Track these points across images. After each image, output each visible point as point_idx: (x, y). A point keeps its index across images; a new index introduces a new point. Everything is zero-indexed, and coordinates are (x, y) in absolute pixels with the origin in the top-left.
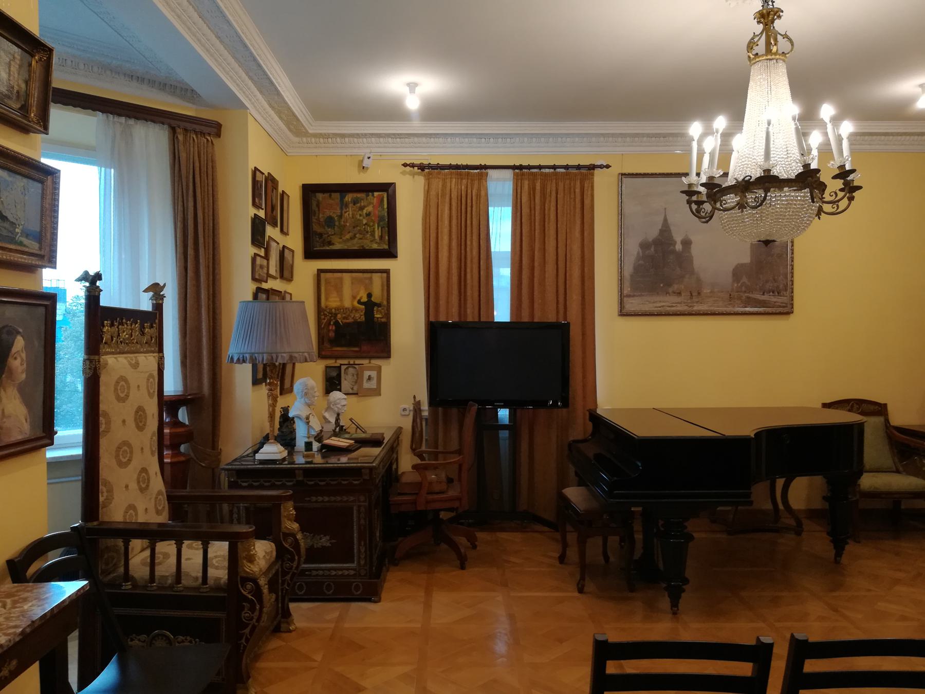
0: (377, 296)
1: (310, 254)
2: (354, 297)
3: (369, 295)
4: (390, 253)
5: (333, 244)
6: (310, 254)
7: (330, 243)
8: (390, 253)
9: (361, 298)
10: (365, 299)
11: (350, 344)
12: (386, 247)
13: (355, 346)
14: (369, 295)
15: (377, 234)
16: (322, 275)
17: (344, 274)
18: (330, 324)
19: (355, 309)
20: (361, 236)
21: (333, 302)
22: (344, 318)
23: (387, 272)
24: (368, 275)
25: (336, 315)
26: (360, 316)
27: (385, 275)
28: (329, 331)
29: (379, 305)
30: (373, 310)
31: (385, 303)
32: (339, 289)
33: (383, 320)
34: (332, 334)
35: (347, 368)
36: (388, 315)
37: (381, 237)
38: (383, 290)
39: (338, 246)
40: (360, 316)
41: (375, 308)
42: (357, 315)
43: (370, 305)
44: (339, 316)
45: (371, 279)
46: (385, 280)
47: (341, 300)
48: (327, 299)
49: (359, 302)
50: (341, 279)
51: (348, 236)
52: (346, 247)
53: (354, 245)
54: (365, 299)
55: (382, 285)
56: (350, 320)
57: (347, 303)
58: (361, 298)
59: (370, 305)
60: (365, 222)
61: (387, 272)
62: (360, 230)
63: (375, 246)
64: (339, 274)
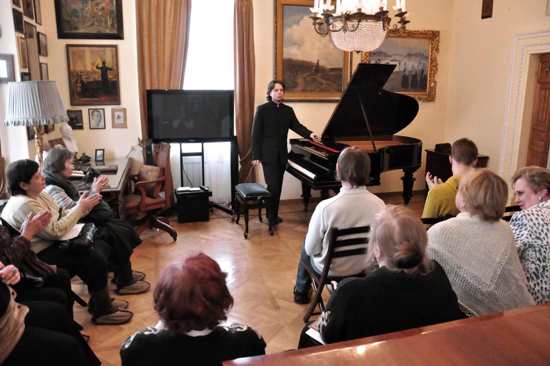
1: (62, 35)
2: (93, 64)
3: (104, 63)
4: (119, 36)
5: (78, 29)
6: (62, 35)
7: (76, 28)
8: (119, 36)
9: (98, 64)
10: (101, 65)
11: (92, 96)
12: (116, 32)
13: (95, 97)
14: (104, 63)
15: (109, 23)
16: (70, 48)
17: (86, 48)
18: (77, 82)
19: (94, 72)
21: (79, 68)
23: (116, 47)
25: (81, 76)
26: (98, 77)
27: (114, 49)
29: (111, 69)
31: (115, 68)
32: (81, 57)
33: (114, 79)
34: (79, 89)
35: (93, 112)
36: (117, 75)
37: (112, 25)
38: (113, 59)
39: (81, 31)
40: (98, 77)
41: (108, 72)
42: (96, 76)
43: (104, 70)
44: (83, 77)
45: (104, 51)
46: (114, 52)
47: (85, 66)
48: (74, 65)
49: (97, 67)
50: (83, 52)
51: (89, 24)
52: (87, 32)
54: (101, 65)
55: (113, 55)
56: (91, 80)
57: (89, 68)
58: (98, 64)
59: (104, 70)
60: (100, 14)
61: (116, 47)
63: (108, 31)
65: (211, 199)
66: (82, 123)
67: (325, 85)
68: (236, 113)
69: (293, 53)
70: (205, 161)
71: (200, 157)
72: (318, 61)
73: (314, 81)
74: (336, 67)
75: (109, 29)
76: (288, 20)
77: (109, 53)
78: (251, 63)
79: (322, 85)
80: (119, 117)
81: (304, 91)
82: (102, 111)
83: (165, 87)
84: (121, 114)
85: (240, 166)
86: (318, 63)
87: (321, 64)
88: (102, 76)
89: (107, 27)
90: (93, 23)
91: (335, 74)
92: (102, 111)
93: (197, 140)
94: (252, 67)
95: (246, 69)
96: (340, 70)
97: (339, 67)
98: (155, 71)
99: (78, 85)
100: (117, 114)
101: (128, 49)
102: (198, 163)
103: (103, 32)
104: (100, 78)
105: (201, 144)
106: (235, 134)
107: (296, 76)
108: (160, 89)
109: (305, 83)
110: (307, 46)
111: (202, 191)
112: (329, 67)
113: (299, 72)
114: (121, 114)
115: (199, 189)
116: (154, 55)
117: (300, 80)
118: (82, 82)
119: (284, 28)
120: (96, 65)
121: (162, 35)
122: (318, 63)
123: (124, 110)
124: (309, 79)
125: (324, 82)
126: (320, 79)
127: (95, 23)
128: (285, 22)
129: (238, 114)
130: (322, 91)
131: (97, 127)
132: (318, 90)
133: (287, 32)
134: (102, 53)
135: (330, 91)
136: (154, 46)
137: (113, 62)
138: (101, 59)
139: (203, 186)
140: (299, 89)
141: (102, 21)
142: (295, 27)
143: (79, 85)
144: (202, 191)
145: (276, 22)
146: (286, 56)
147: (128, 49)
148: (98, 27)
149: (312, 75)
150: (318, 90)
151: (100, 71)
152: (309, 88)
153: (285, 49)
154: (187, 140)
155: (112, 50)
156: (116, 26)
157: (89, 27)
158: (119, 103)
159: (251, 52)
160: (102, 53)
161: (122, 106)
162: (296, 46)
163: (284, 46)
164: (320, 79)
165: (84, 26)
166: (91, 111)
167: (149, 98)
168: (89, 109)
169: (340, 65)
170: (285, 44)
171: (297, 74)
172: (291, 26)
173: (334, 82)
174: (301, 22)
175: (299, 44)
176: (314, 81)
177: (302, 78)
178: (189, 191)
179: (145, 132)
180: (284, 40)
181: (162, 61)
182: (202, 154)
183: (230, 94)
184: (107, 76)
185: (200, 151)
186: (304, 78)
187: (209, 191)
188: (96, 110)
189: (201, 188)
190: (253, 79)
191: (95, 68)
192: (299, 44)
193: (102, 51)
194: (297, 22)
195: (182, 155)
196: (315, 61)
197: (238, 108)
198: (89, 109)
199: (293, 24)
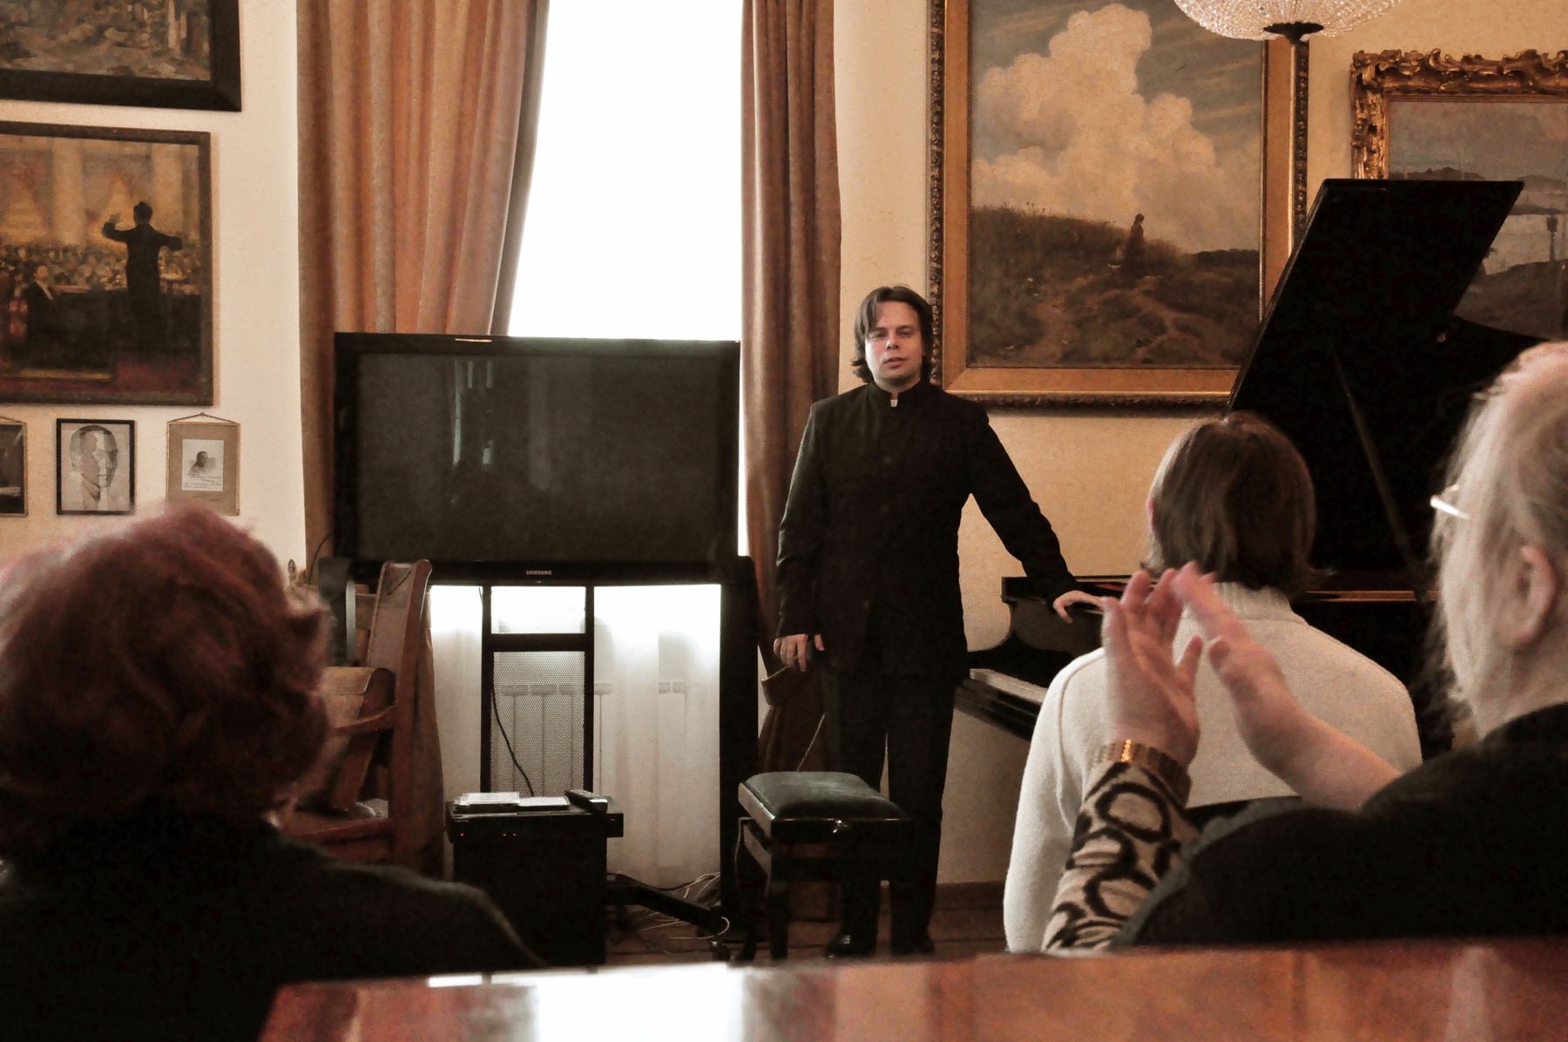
0: (168, 216)
2: (91, 216)
3: (143, 212)
5: (27, 55)
7: (15, 50)
8: (222, 92)
10: (127, 223)
12: (204, 75)
14: (143, 212)
15: (175, 34)
17: (59, 142)
19: (91, 252)
20: (121, 37)
22: (58, 279)
23: (201, 141)
24: (140, 148)
25: (31, 267)
26: (110, 274)
27: (193, 150)
28: (8, 317)
29: (174, 243)
30: (155, 258)
31: (194, 236)
33: (188, 289)
34: (18, 328)
36: (203, 271)
37: (188, 46)
38: (185, 198)
39: (40, 63)
40: (110, 274)
41: (163, 253)
42: (104, 273)
43: (144, 243)
44: (42, 271)
45: (148, 157)
46: (194, 168)
47: (49, 222)
49: (110, 231)
50: (47, 157)
51: (76, 33)
52: (69, 68)
53: (100, 63)
54: (127, 223)
55: (185, 180)
56: (80, 286)
57: (70, 236)
59: (144, 243)
61: (201, 141)
62: (116, 17)
63: (167, 71)
64: (42, 142)
65: (623, 855)
66: (21, 482)
67: (1173, 333)
68: (750, 454)
69: (1015, 182)
70: (598, 681)
71: (577, 657)
72: (1139, 218)
73: (1121, 311)
74: (1227, 249)
75: (172, 61)
76: (992, 35)
77: (168, 165)
78: (823, 224)
79: (1162, 329)
80: (201, 461)
81: (1073, 358)
82: (121, 433)
83: (419, 321)
84: (214, 448)
85: (764, 709)
86: (1137, 229)
87: (1158, 230)
88: (129, 269)
89: (162, 53)
90: (100, 31)
91: (1225, 280)
92: (121, 433)
93: (561, 575)
94: (825, 242)
95: (796, 252)
96: (1247, 259)
97: (1241, 247)
98: (378, 253)
99: (13, 308)
100: (191, 448)
101: (257, 155)
102: (566, 691)
103: (144, 74)
104: (122, 280)
105: (580, 591)
106: (743, 549)
107: (1030, 291)
108: (401, 329)
109: (1079, 325)
110: (1087, 150)
111: (576, 811)
112: (1189, 246)
113: (1047, 273)
114: (214, 448)
115: (562, 801)
116: (377, 179)
117: (1052, 311)
118: (34, 294)
119: (978, 65)
120: (105, 218)
121: (416, 91)
122: (1137, 229)
123: (230, 433)
124: (1093, 302)
125: (1168, 316)
126: (1149, 306)
127: (109, 33)
128: (981, 42)
129: (760, 455)
130: (1161, 358)
131: (92, 506)
132: (1141, 353)
133: (993, 84)
134: (135, 169)
135: (1197, 359)
136: (376, 137)
137: (186, 213)
138: (131, 192)
139: (581, 792)
140: (1049, 346)
141: (142, 25)
142: (1028, 64)
143: (18, 307)
144: (576, 811)
145: (938, 43)
146: (983, 198)
147: (257, 155)
148: (118, 51)
149: (1109, 284)
150: (1141, 353)
151: (123, 246)
152: (1097, 347)
153: (980, 166)
154: (517, 574)
155: (182, 158)
156: (206, 47)
157: (74, 46)
158: (205, 397)
159: (821, 178)
160: (135, 169)
161: (223, 410)
162: (1039, 151)
163: (977, 151)
164: (1149, 306)
165: (53, 44)
166: (69, 432)
167: (348, 374)
168: (60, 422)
169: (1249, 240)
170: (980, 141)
171: (1039, 280)
172: (1006, 62)
173: (1219, 318)
174: (1056, 42)
175: (1049, 142)
176: (1121, 311)
177: (1060, 301)
178: (514, 808)
179: (322, 530)
180: (978, 127)
181: (411, 209)
182: (584, 642)
183: (725, 358)
184: (156, 270)
185: (575, 626)
186: (1072, 302)
187: (610, 810)
188: (94, 424)
189: (575, 800)
190: (829, 302)
191: (98, 236)
192: (1049, 142)
193: (133, 158)
194: (1039, 44)
195: (494, 644)
196: (1124, 223)
197: (760, 429)
198: (60, 422)
199: (1018, 50)
